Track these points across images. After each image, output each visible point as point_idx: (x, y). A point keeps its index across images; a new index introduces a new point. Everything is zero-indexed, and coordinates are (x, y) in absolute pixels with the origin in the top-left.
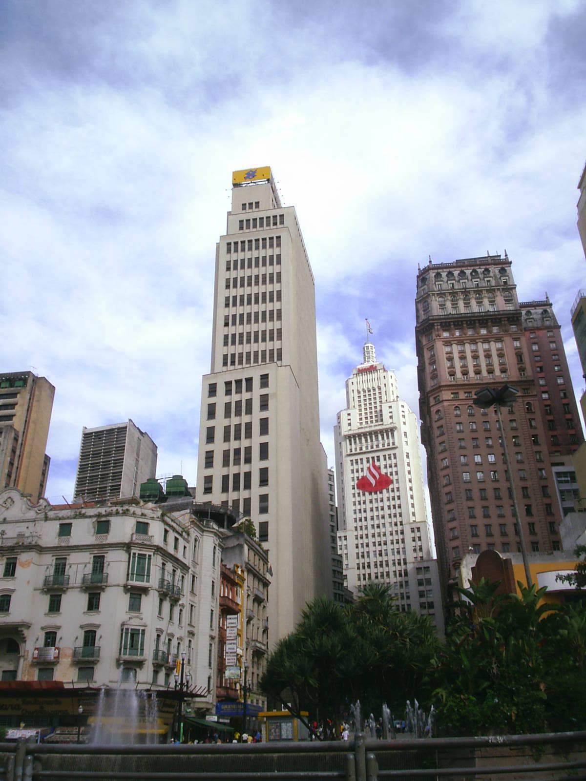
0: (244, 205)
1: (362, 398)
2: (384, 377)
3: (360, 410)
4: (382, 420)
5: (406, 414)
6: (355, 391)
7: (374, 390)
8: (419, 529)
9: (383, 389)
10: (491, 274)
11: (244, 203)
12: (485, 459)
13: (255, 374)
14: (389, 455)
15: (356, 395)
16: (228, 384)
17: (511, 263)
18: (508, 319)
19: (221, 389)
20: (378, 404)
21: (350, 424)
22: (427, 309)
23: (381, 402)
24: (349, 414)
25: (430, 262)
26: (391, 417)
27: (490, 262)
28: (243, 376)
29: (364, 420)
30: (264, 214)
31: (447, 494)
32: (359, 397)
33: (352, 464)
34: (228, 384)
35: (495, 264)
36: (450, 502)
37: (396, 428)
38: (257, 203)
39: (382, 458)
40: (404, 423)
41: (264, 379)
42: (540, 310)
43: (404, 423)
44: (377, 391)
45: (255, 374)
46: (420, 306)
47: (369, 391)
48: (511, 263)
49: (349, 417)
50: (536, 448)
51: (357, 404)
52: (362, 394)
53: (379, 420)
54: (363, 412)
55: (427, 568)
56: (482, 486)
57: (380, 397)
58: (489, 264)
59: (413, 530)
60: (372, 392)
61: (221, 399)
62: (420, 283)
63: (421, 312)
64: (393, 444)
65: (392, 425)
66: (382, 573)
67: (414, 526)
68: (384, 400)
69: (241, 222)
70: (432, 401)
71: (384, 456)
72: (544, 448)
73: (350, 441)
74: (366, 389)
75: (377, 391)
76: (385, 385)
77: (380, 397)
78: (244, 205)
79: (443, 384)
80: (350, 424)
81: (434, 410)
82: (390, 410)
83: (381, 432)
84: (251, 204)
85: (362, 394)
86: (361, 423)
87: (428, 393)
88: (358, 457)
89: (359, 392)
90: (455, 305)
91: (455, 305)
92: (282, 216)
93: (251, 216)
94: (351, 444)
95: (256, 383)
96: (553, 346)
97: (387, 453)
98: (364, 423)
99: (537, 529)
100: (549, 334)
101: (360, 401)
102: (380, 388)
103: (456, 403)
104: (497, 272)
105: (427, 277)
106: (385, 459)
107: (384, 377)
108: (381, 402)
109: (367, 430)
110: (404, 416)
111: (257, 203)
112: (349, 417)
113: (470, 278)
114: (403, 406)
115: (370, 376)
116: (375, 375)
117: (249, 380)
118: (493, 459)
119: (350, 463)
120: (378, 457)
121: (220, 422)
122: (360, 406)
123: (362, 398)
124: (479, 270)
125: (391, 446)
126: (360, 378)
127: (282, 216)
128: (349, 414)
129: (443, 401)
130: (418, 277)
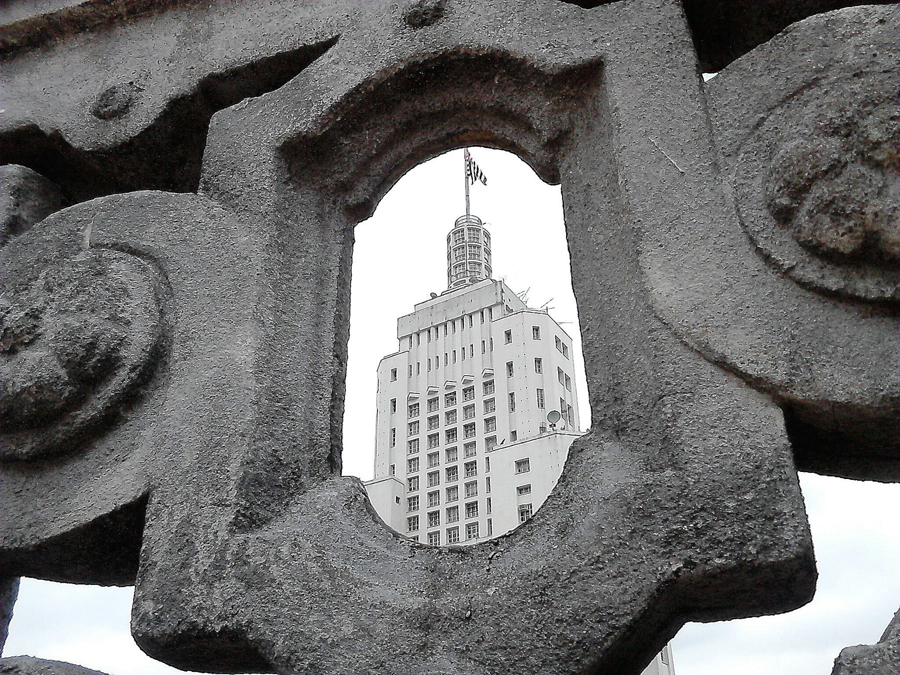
1: (424, 433)
2: (508, 334)
3: (413, 482)
7: (468, 391)
15: (402, 418)
44: (479, 399)
47: (451, 398)
51: (401, 457)
52: (424, 415)
60: (460, 404)
68: (502, 432)
75: (479, 399)
76: (510, 366)
82: (523, 480)
85: (424, 415)
89: (413, 408)
101: (413, 444)
102: (488, 385)
107: (508, 334)
108: (490, 440)
115: (457, 339)
116: (476, 331)
122: (413, 463)
126: (423, 350)
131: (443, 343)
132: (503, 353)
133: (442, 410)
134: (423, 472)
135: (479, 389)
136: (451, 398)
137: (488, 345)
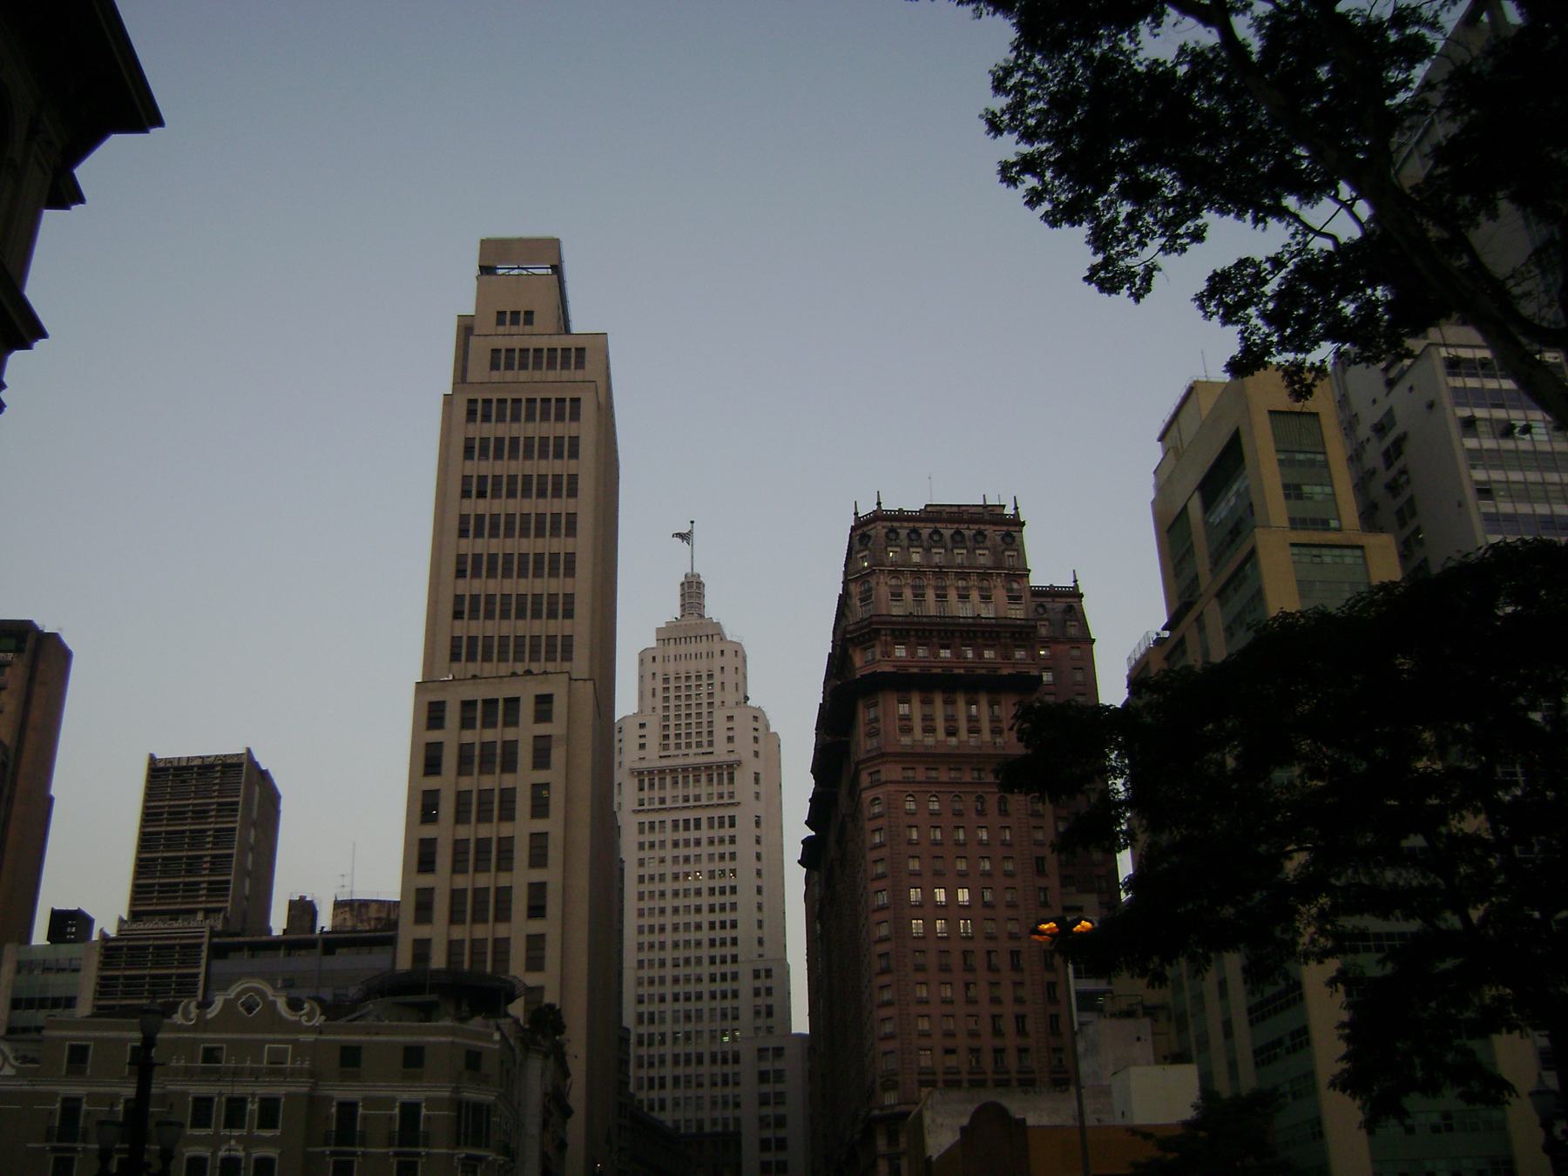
0: (501, 314)
1: (672, 694)
3: (666, 718)
4: (711, 743)
5: (759, 734)
6: (659, 678)
7: (699, 677)
8: (768, 973)
9: (717, 681)
10: (988, 543)
11: (501, 309)
12: (951, 896)
13: (526, 691)
14: (721, 818)
15: (659, 685)
16: (468, 705)
17: (1023, 524)
18: (1013, 634)
19: (452, 716)
20: (705, 710)
21: (642, 746)
22: (866, 598)
23: (711, 704)
24: (642, 726)
25: (879, 504)
26: (730, 739)
27: (987, 517)
28: (502, 692)
29: (672, 741)
30: (544, 343)
31: (880, 956)
32: (666, 689)
33: (641, 831)
34: (468, 705)
35: (995, 524)
36: (885, 971)
37: (739, 763)
38: (529, 314)
39: (704, 824)
40: (756, 754)
41: (544, 701)
42: (1060, 604)
43: (756, 754)
44: (705, 681)
45: (526, 691)
46: (855, 589)
47: (688, 678)
48: (1023, 524)
49: (643, 732)
50: (1042, 882)
51: (659, 704)
52: (672, 685)
53: (705, 743)
54: (672, 723)
55: (778, 1052)
56: (944, 946)
57: (710, 695)
58: (985, 523)
59: (756, 974)
60: (693, 683)
61: (450, 736)
62: (857, 546)
63: (856, 602)
64: (731, 795)
65: (732, 757)
66: (688, 1056)
67: (761, 966)
68: (717, 700)
69: (496, 352)
70: (865, 779)
71: (711, 819)
72: (1053, 882)
73: (641, 782)
74: (683, 676)
75: (705, 681)
77: (710, 695)
78: (501, 314)
79: (890, 750)
80: (642, 746)
81: (867, 796)
82: (730, 725)
83: (708, 767)
84: (515, 314)
86: (666, 747)
87: (858, 763)
88: (656, 818)
89: (666, 680)
90: (919, 596)
91: (919, 596)
92: (581, 351)
93: (516, 343)
94: (641, 789)
95: (527, 709)
96: (1079, 677)
97: (716, 813)
98: (672, 746)
99: (1030, 1025)
100: (1075, 652)
101: (666, 699)
102: (710, 676)
103: (910, 789)
104: (998, 539)
105: (872, 533)
106: (711, 826)
108: (711, 704)
109: (680, 761)
110: (756, 739)
111: (529, 314)
112: (643, 732)
113: (949, 545)
114: (756, 718)
115: (692, 648)
116: (704, 646)
117: (513, 703)
118: (967, 898)
119: (635, 828)
120: (698, 822)
121: (447, 783)
122: (666, 708)
123: (672, 694)
124: (966, 532)
125: (726, 800)
126: (672, 649)
127: (581, 351)
128: (642, 726)
129: (886, 782)
130: (853, 529)
131: (683, 649)
132: (718, 661)
133: (683, 684)
134: (672, 713)
135: (704, 677)
136: (688, 678)
137: (710, 655)
